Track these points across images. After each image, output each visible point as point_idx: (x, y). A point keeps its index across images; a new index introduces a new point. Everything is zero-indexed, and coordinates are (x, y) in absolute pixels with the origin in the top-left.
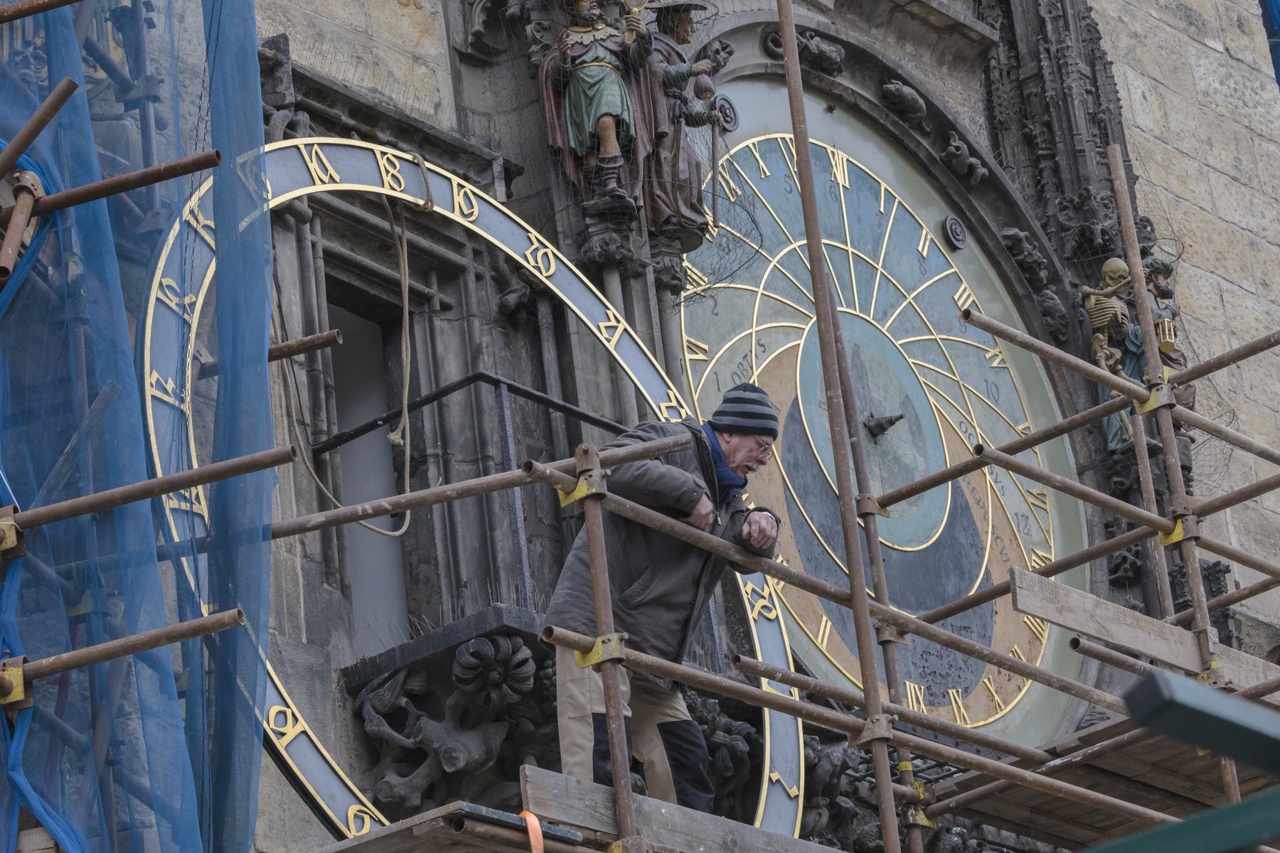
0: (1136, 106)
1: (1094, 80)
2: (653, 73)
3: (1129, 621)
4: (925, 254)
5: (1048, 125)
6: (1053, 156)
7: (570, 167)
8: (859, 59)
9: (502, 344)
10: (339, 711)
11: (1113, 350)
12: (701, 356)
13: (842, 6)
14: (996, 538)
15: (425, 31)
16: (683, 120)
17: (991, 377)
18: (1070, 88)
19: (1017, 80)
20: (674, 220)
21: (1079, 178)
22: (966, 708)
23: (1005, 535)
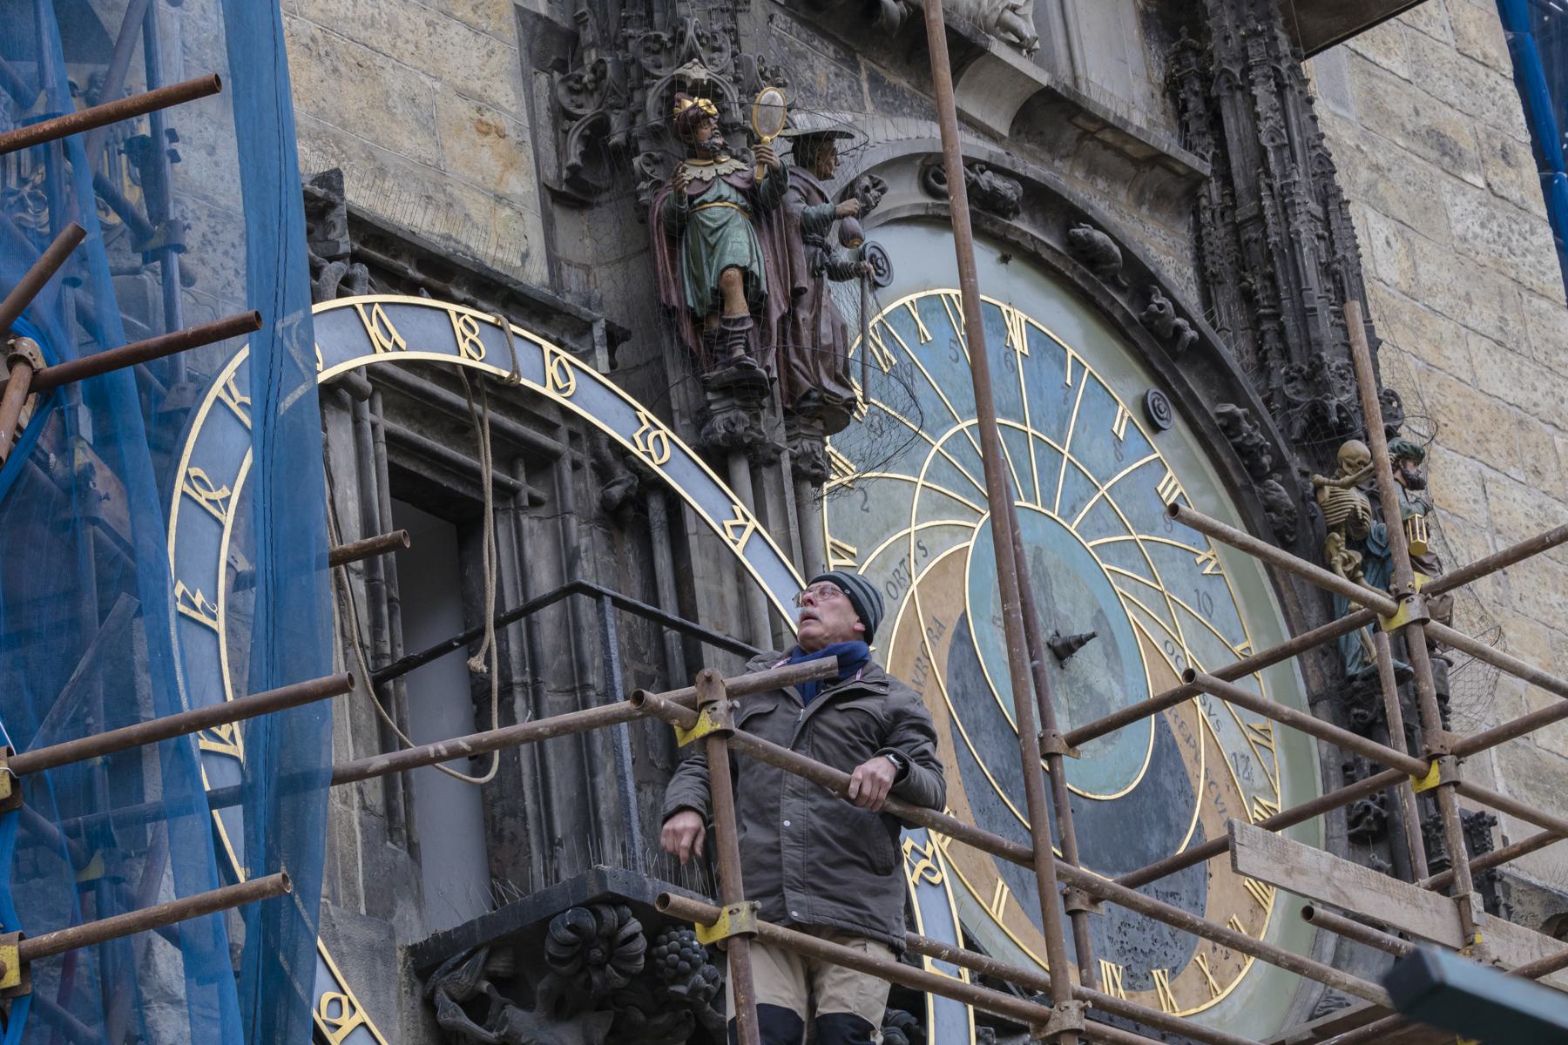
0: (1379, 254)
1: (1327, 223)
2: (788, 216)
3: (1374, 884)
5: (1272, 278)
6: (1278, 316)
7: (687, 330)
8: (1040, 198)
9: (604, 548)
10: (406, 999)
11: (1352, 553)
13: (1019, 132)
14: (1210, 783)
15: (510, 165)
16: (825, 272)
17: (1203, 586)
18: (1298, 233)
19: (1233, 223)
20: (815, 395)
21: (1309, 343)
22: (1174, 992)
23: (1221, 780)
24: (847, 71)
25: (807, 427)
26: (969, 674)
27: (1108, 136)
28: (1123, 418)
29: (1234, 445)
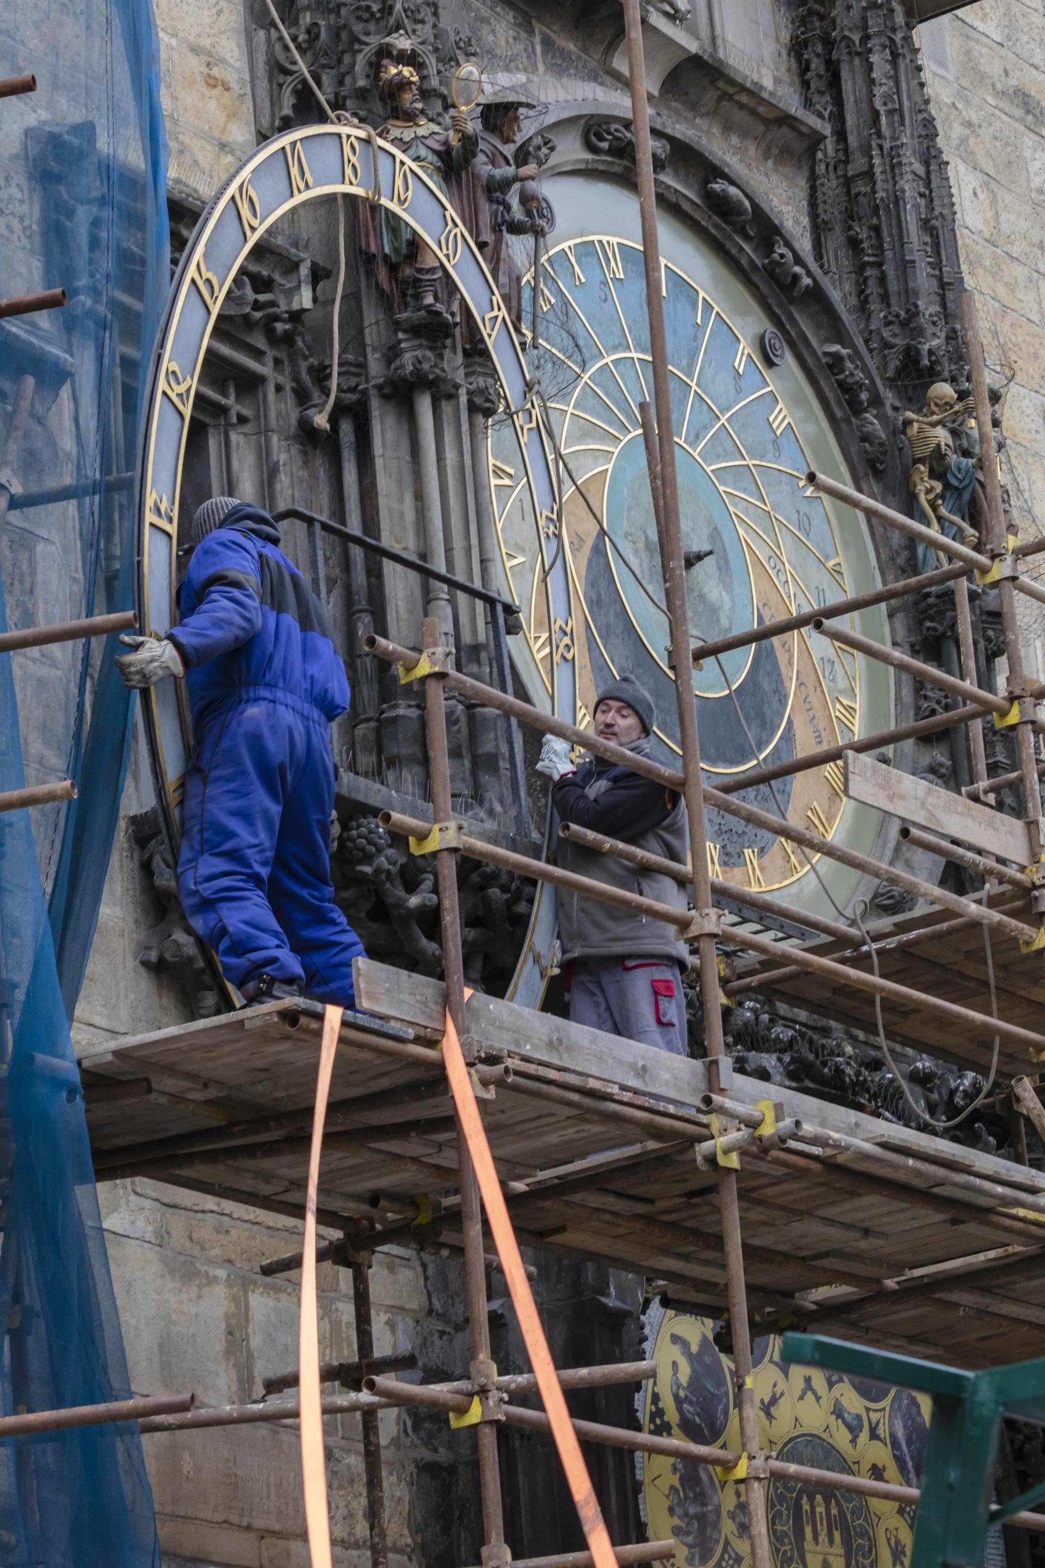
0: (966, 203)
1: (928, 182)
2: (475, 176)
3: (960, 809)
4: (741, 371)
5: (877, 229)
6: (880, 264)
7: (383, 275)
8: (683, 155)
9: (300, 462)
10: (126, 862)
12: (506, 482)
13: (667, 93)
14: (801, 684)
15: (233, 115)
16: (504, 228)
17: (804, 507)
18: (903, 191)
19: (845, 176)
21: (907, 292)
22: (762, 869)
23: (810, 682)
24: (523, 35)
25: (481, 365)
26: (603, 583)
27: (744, 99)
28: (744, 352)
29: (837, 381)
